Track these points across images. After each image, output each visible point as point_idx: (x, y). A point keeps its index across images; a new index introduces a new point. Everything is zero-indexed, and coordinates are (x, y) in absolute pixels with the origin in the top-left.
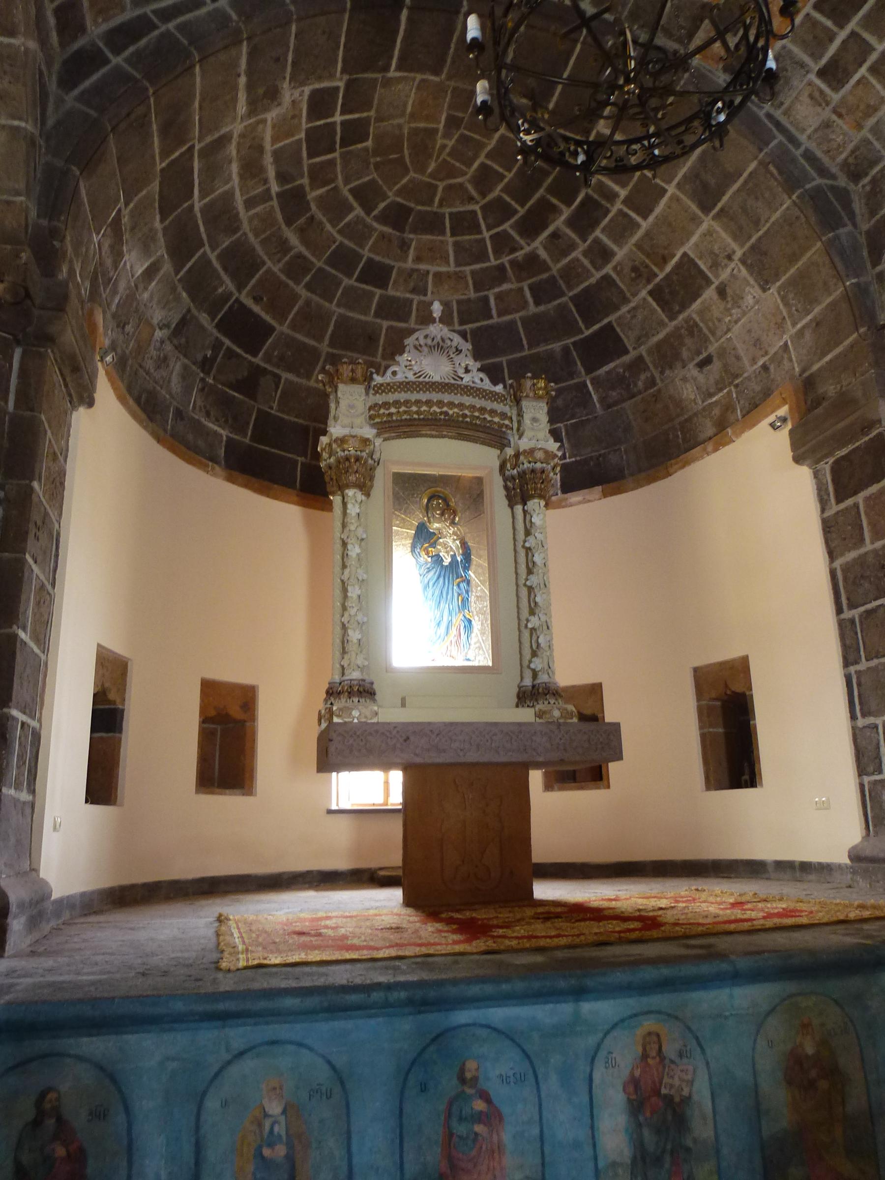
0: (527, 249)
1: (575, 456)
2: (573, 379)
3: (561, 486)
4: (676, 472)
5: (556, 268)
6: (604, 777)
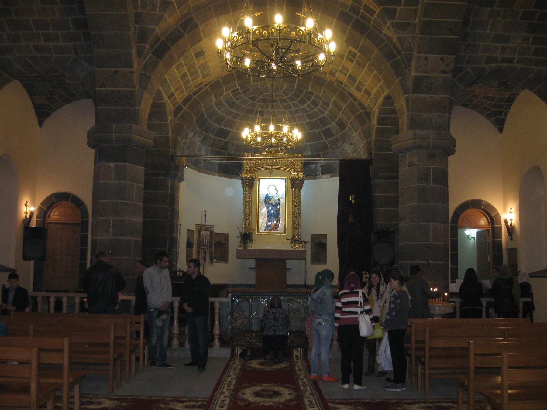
5: (312, 112)
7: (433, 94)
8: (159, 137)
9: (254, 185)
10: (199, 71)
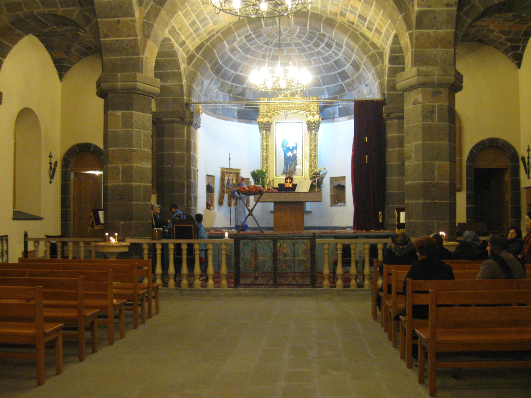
0: (317, 50)
5: (327, 54)
7: (437, 29)
8: (174, 85)
9: (272, 129)
10: (208, 17)
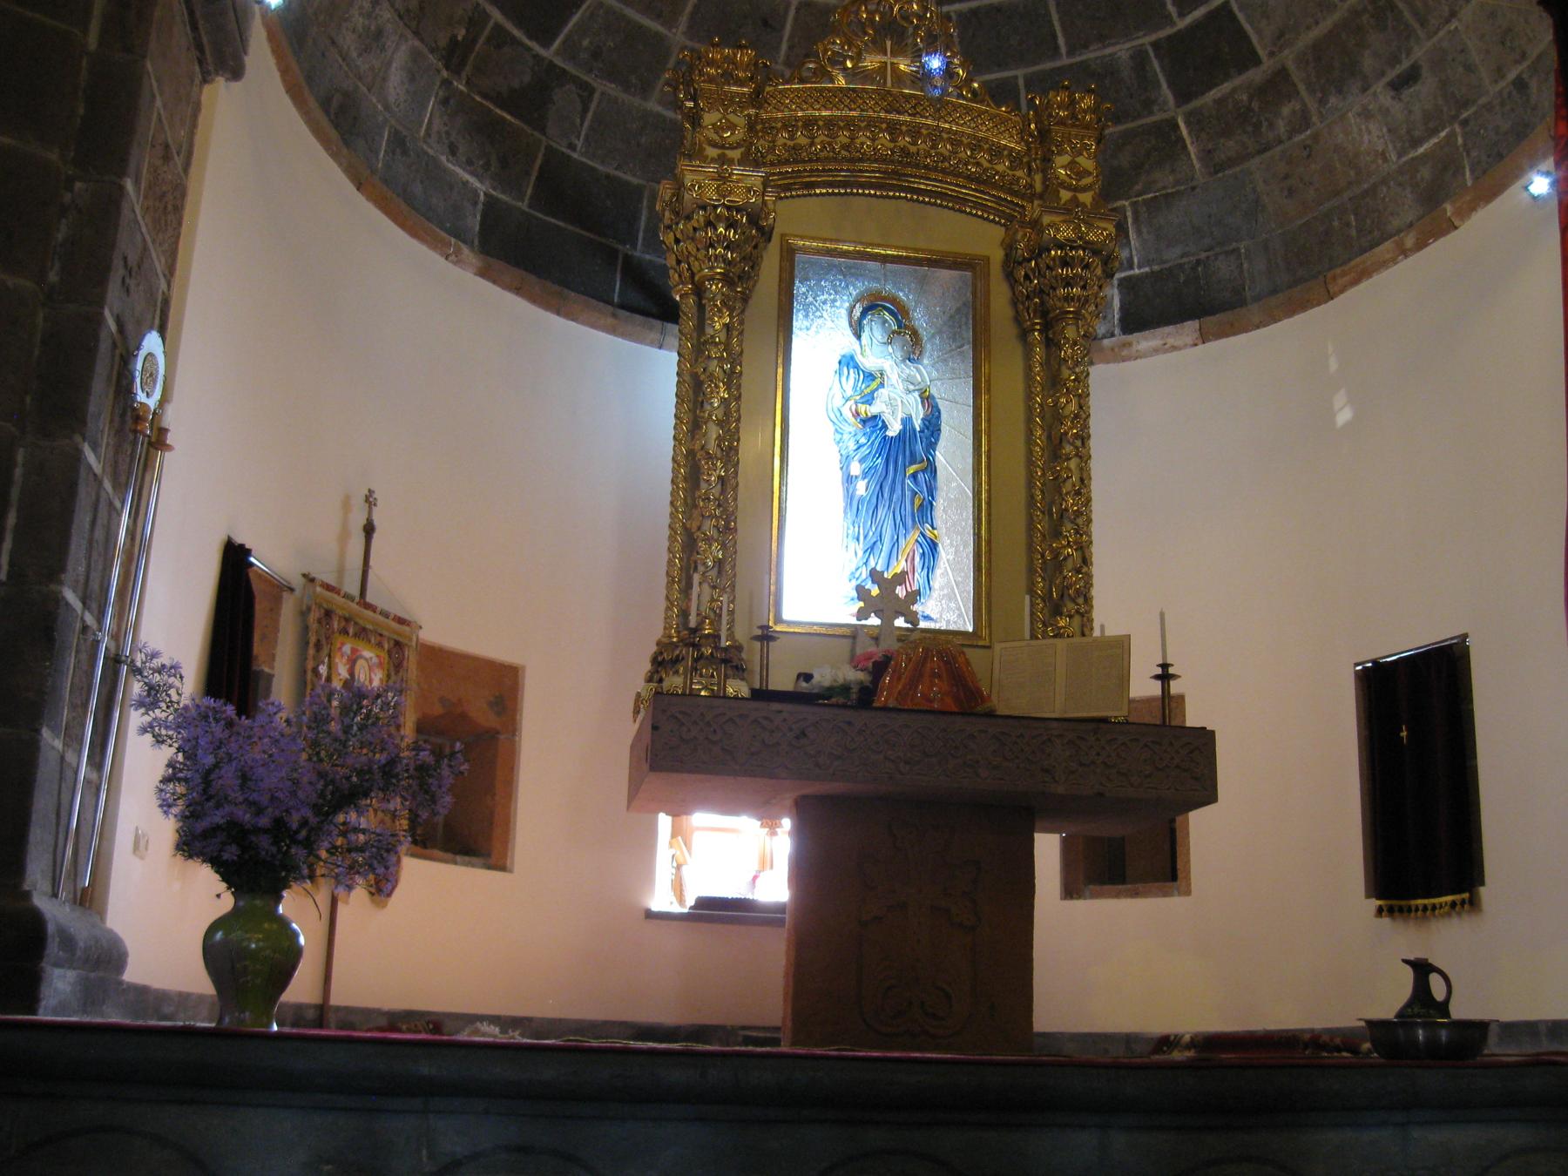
1: (1149, 262)
2: (1151, 113)
3: (1121, 320)
4: (1342, 291)
6: (1180, 875)
